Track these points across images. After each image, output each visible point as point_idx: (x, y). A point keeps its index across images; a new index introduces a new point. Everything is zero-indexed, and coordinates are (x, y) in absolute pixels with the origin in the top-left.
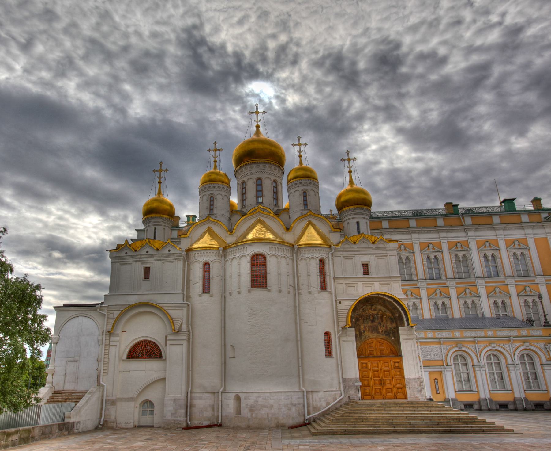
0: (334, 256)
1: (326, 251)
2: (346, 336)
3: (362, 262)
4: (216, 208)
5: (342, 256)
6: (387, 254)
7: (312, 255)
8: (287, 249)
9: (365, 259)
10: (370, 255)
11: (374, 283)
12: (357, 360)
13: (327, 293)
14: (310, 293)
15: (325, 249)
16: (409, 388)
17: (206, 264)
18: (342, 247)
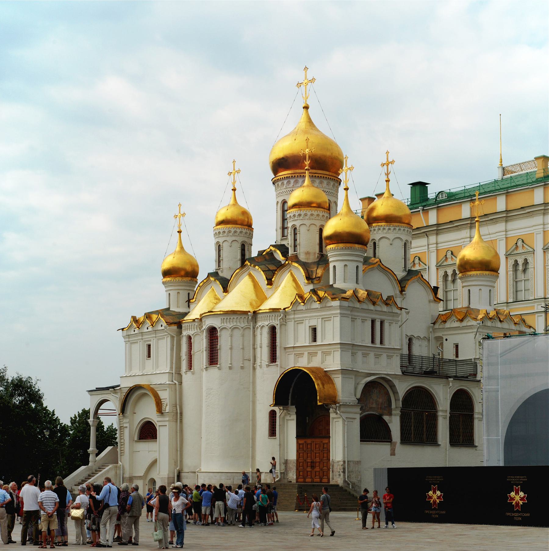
0: (287, 321)
1: (278, 316)
2: (289, 414)
3: (310, 326)
4: (222, 260)
5: (293, 320)
6: (332, 314)
7: (262, 323)
8: (243, 318)
9: (313, 323)
10: (317, 318)
11: (317, 352)
12: (295, 440)
13: (276, 366)
14: (261, 366)
15: (276, 314)
16: (333, 471)
17: (190, 338)
18: (293, 310)
